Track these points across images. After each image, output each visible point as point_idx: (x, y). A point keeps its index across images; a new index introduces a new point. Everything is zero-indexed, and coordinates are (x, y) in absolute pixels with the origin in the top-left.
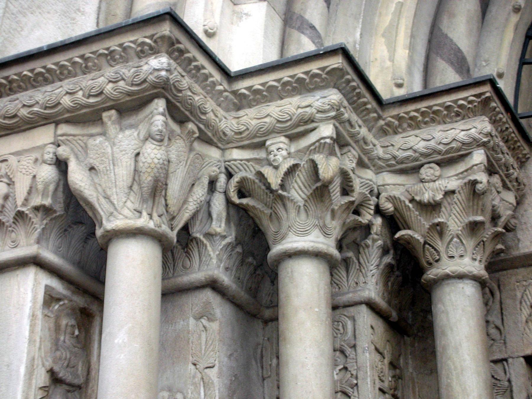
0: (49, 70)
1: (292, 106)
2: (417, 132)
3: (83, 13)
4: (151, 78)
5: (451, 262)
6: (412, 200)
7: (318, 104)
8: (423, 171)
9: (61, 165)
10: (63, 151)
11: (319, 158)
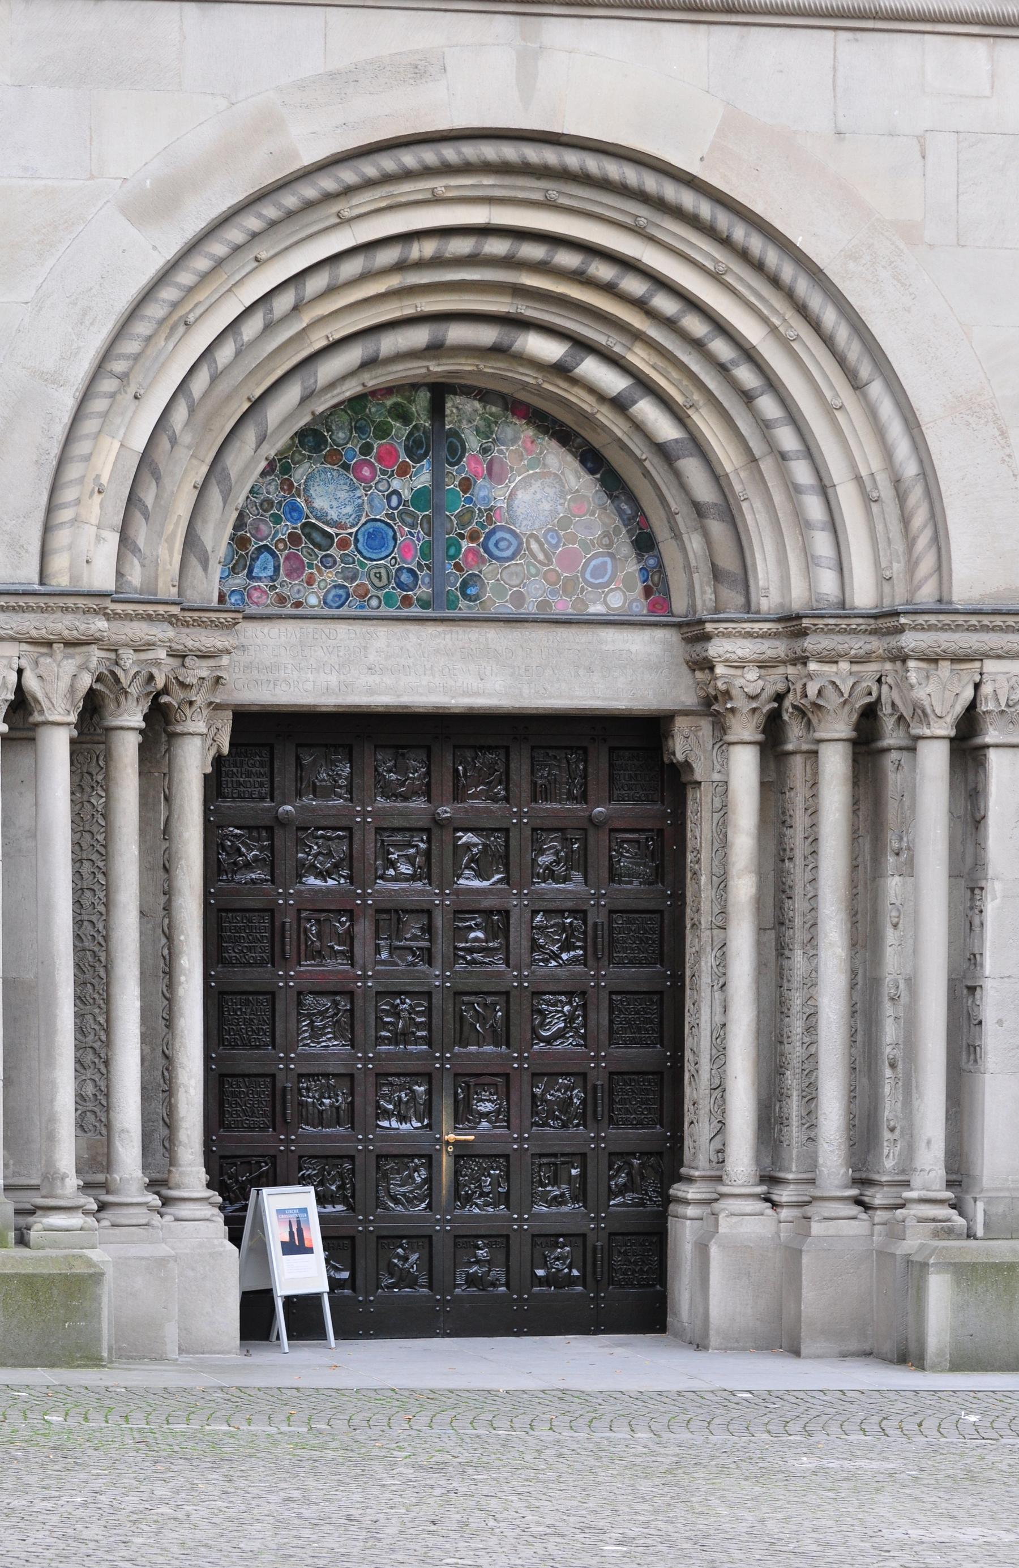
0: (19, 606)
1: (140, 631)
2: (187, 631)
3: (27, 551)
4: (98, 635)
5: (193, 724)
6: (176, 678)
7: (160, 636)
8: (187, 660)
9: (20, 672)
10: (24, 663)
11: (155, 671)
